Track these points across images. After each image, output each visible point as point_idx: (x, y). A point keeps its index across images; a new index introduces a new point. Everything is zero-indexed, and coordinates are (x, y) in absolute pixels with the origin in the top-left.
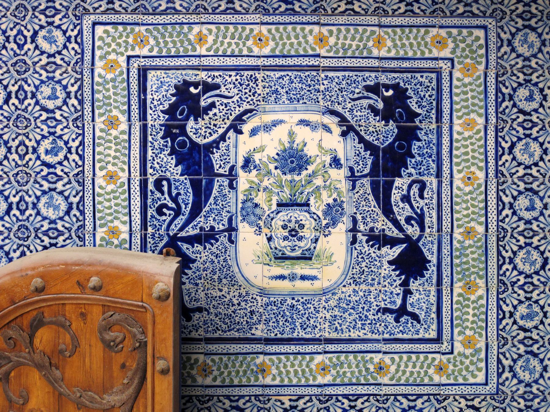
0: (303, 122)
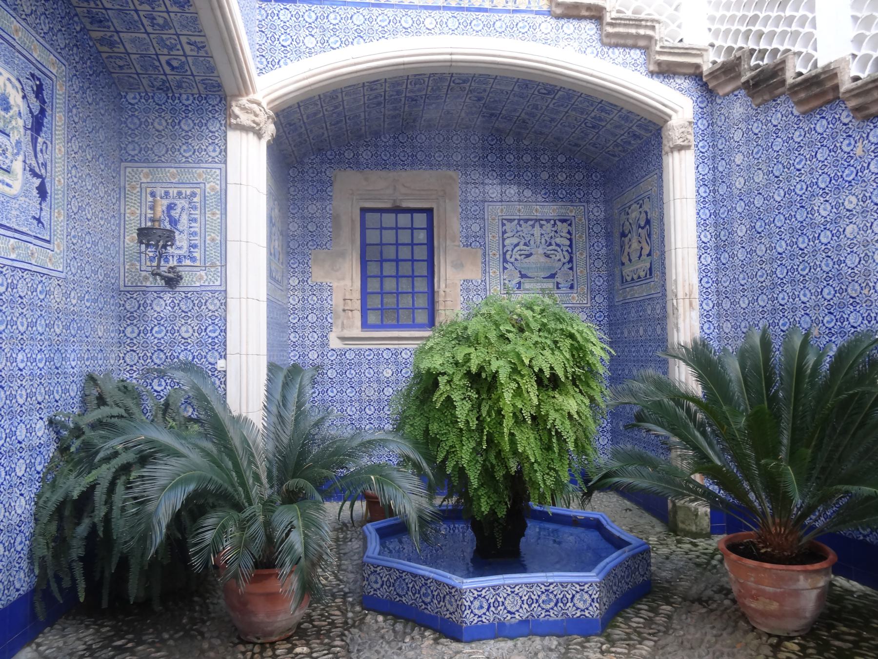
0: (9, 79)
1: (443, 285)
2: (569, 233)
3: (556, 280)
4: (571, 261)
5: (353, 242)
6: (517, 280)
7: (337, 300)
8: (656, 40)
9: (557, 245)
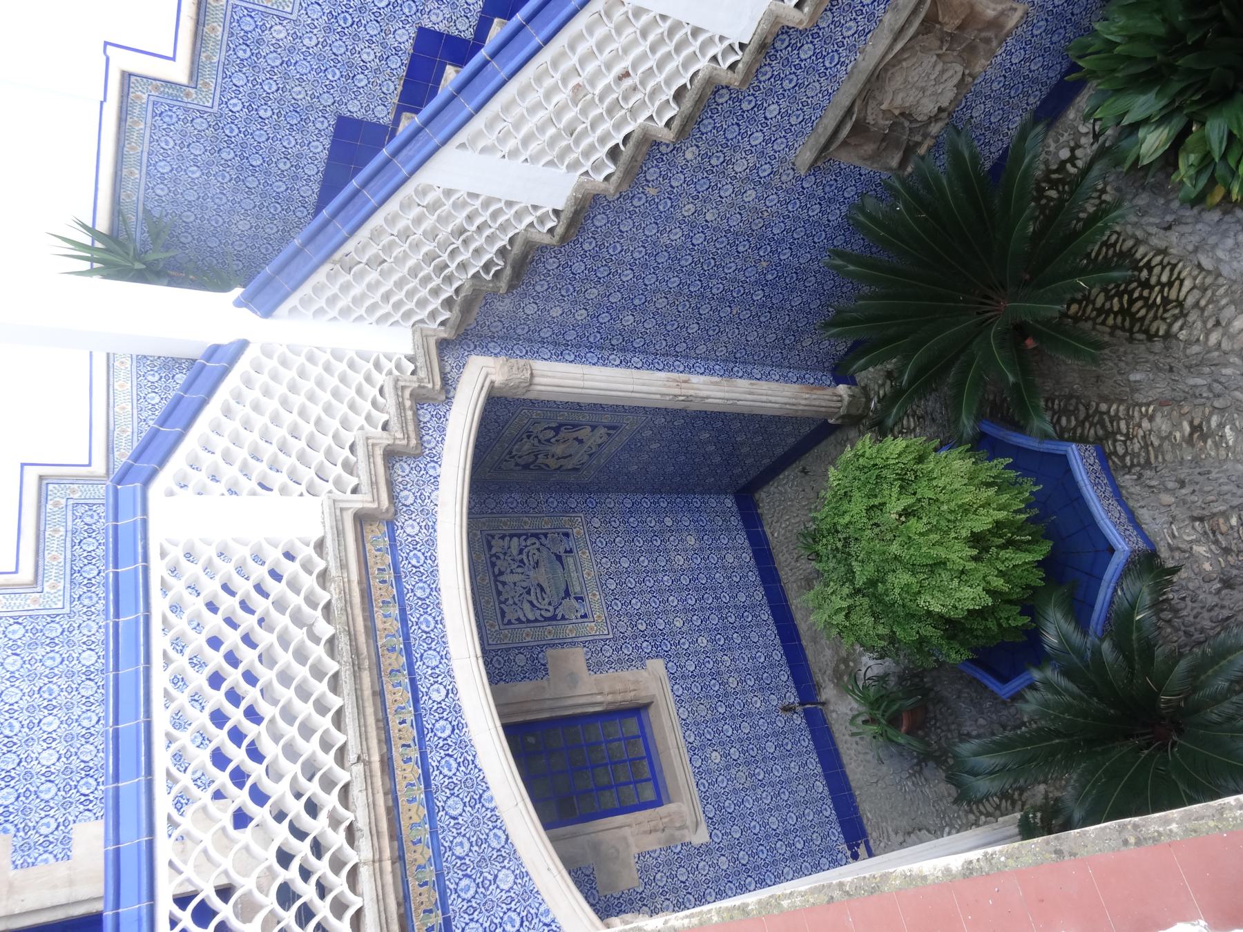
1: (599, 698)
2: (503, 538)
3: (562, 554)
4: (536, 536)
5: (574, 835)
6: (573, 602)
7: (652, 843)
8: (420, 387)
9: (521, 552)
